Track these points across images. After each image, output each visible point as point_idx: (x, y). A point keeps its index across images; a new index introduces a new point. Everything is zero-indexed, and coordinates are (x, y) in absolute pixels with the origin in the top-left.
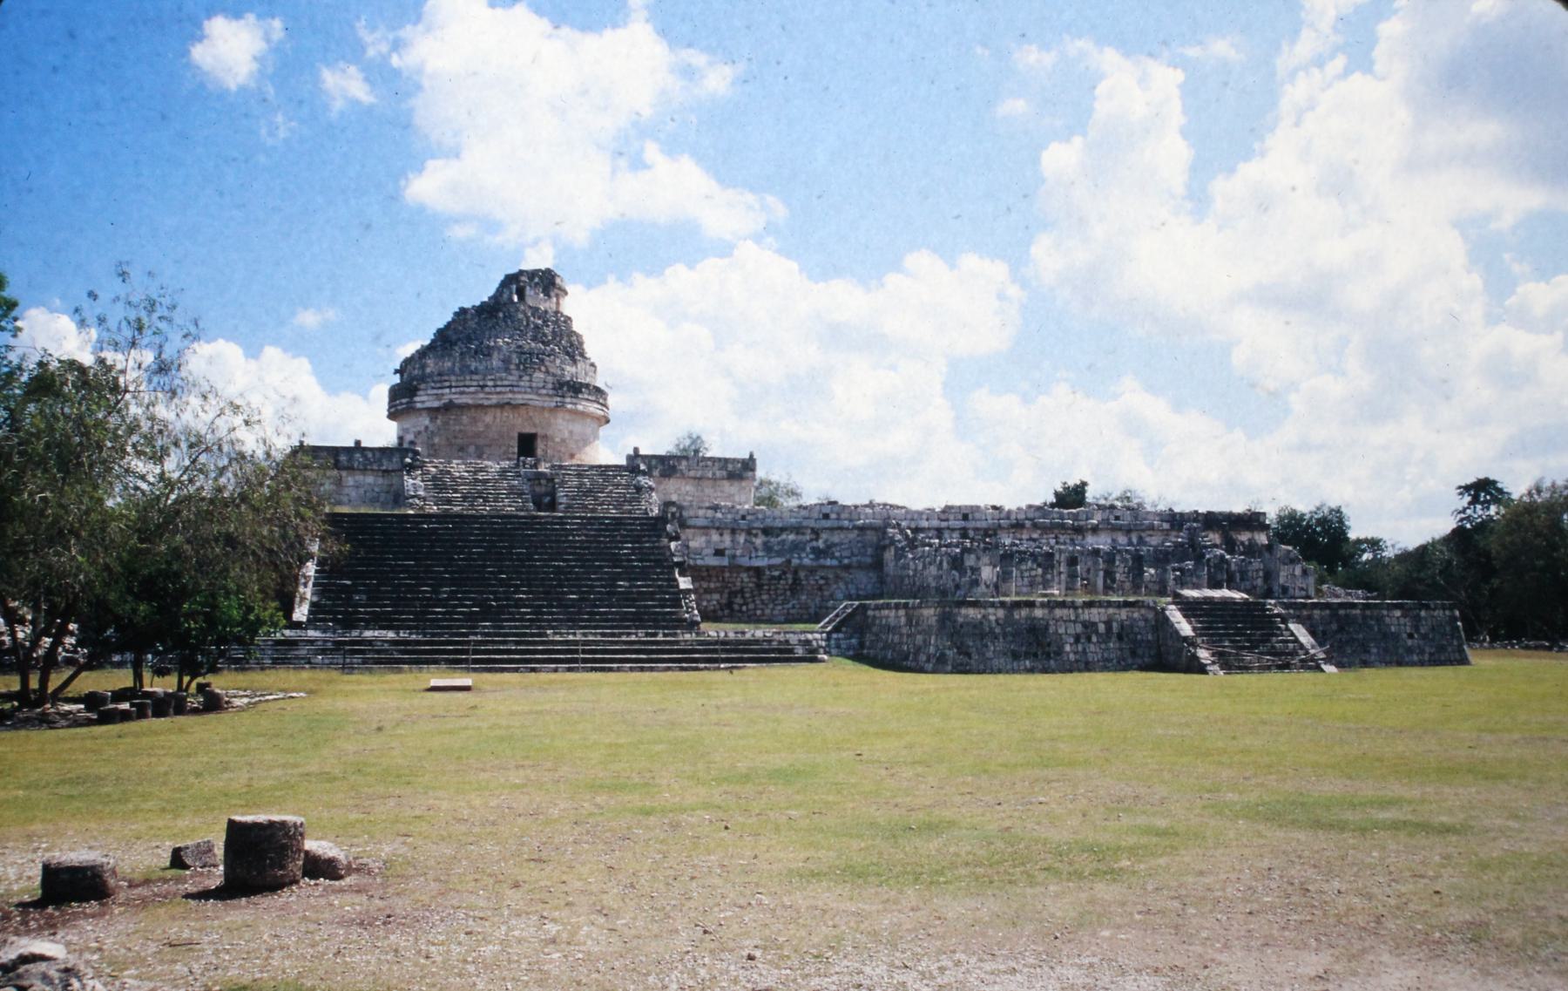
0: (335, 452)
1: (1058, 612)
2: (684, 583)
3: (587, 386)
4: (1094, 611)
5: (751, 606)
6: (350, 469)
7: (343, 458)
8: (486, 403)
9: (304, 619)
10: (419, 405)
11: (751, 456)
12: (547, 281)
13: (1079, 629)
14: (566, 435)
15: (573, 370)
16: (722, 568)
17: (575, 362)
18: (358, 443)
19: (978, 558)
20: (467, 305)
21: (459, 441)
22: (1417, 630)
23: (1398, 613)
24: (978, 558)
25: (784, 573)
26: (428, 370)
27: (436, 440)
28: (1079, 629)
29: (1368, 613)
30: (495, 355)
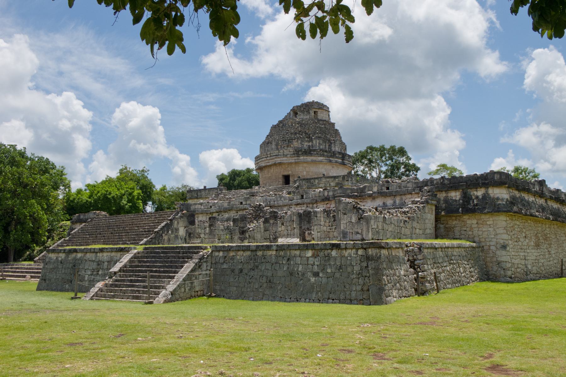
1: (89, 256)
3: (314, 150)
4: (105, 254)
7: (199, 194)
8: (268, 164)
13: (94, 266)
14: (305, 173)
15: (310, 144)
17: (311, 140)
18: (205, 187)
19: (178, 223)
20: (275, 124)
22: (323, 270)
23: (309, 253)
24: (178, 223)
28: (94, 266)
29: (282, 253)
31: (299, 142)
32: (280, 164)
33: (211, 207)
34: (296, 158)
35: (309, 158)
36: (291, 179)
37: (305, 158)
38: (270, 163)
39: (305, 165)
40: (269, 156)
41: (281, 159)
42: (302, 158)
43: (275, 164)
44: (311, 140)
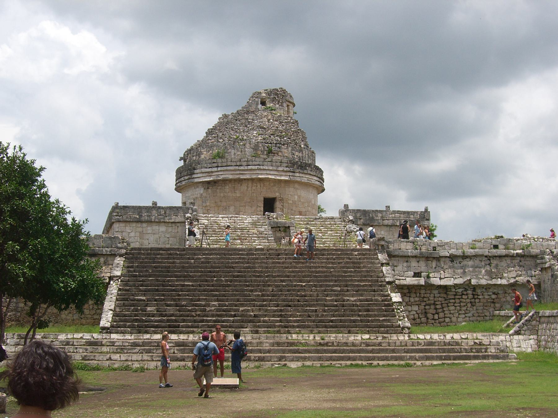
0: (139, 209)
2: (396, 297)
5: (441, 315)
6: (150, 222)
8: (242, 177)
9: (108, 325)
10: (196, 180)
11: (426, 210)
12: (279, 96)
14: (296, 197)
15: (300, 155)
16: (419, 287)
18: (155, 203)
21: (225, 204)
25: (466, 290)
26: (203, 156)
27: (208, 204)
30: (248, 145)
31: (290, 149)
32: (261, 180)
33: (434, 249)
34: (291, 174)
35: (305, 178)
36: (278, 205)
37: (301, 175)
38: (248, 177)
39: (296, 186)
40: (245, 163)
41: (268, 172)
42: (297, 175)
43: (252, 180)
44: (301, 151)
